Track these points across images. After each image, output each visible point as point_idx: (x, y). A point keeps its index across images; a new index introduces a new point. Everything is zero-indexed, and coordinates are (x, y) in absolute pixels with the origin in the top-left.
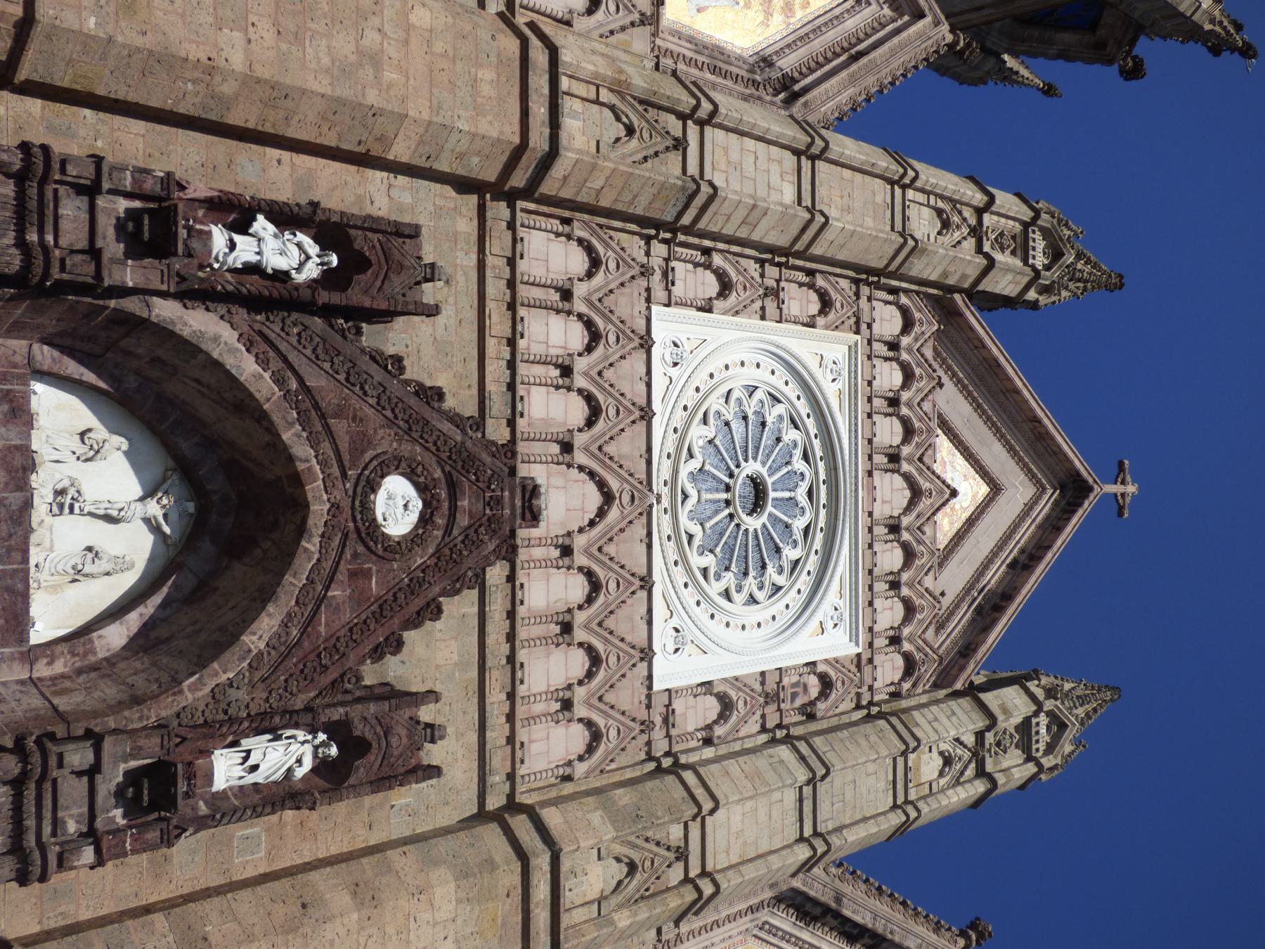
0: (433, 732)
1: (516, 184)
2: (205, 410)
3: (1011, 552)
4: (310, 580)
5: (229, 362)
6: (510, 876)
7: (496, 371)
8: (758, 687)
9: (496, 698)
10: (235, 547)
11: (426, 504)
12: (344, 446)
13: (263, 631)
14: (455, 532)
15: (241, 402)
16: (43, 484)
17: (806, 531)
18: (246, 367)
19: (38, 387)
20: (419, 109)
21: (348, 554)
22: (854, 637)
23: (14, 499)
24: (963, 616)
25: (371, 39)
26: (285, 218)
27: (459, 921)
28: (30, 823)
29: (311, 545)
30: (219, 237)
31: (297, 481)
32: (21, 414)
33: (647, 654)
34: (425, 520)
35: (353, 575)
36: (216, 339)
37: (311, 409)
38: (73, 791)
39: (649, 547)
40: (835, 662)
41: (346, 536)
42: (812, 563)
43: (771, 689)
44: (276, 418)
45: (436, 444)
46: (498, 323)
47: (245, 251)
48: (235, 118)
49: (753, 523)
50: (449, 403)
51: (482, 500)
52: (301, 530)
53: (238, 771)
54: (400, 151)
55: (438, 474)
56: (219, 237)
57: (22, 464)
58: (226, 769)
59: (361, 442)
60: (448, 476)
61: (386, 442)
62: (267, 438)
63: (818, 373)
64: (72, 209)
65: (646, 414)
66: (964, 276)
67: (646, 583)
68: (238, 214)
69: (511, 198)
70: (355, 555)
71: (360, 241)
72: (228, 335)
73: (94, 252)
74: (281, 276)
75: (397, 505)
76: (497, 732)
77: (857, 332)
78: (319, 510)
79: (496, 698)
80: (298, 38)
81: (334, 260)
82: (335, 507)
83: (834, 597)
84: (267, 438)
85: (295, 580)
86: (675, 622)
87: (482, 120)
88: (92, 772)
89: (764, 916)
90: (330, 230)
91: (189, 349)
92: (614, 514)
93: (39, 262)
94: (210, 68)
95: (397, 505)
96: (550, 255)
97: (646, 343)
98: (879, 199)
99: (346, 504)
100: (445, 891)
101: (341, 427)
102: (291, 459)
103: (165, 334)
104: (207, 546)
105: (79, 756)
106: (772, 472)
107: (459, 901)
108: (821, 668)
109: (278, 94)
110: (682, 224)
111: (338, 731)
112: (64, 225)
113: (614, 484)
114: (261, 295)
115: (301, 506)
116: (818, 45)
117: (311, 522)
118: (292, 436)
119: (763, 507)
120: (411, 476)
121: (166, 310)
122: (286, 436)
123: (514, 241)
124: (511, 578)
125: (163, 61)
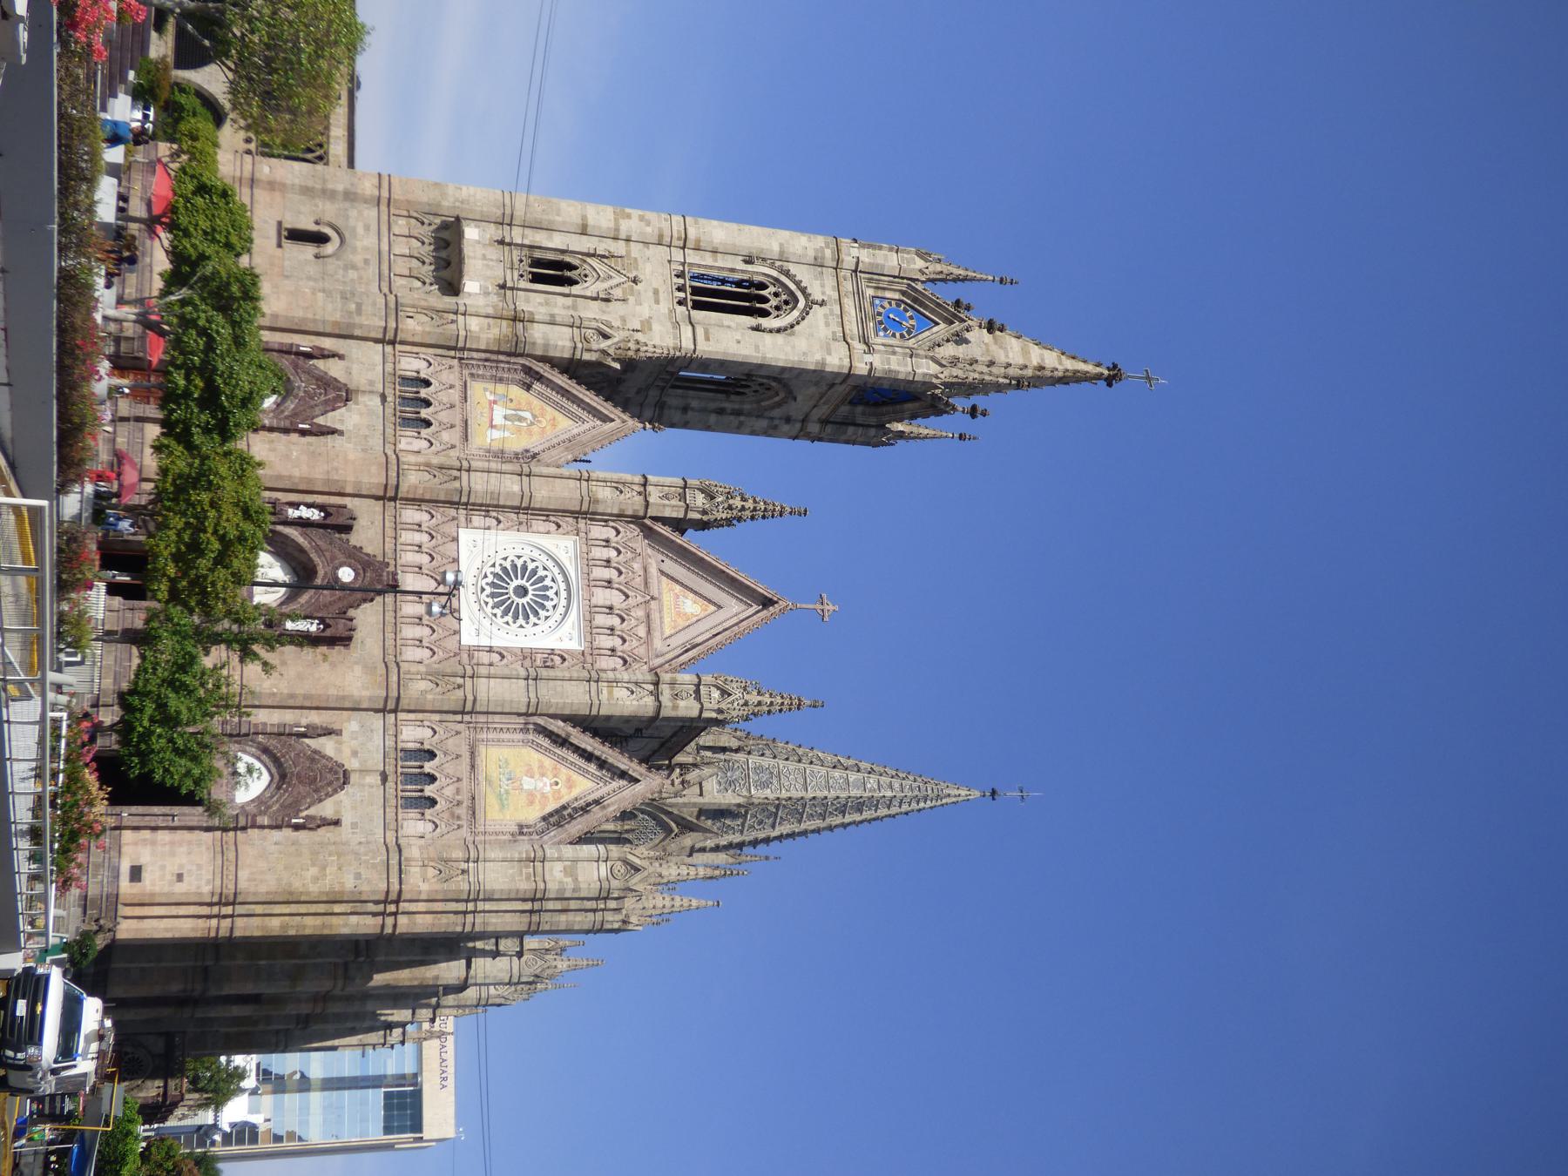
1: (389, 496)
2: (296, 554)
3: (720, 628)
6: (381, 669)
7: (389, 546)
9: (390, 636)
13: (304, 598)
15: (302, 550)
18: (301, 540)
20: (351, 478)
24: (679, 651)
26: (309, 506)
30: (290, 511)
33: (457, 632)
37: (319, 549)
40: (567, 651)
42: (557, 617)
43: (527, 655)
46: (390, 532)
48: (301, 487)
49: (524, 600)
54: (349, 490)
58: (289, 625)
65: (456, 560)
68: (296, 505)
69: (390, 499)
71: (330, 510)
75: (346, 575)
76: (390, 643)
87: (373, 478)
89: (531, 737)
90: (321, 508)
91: (286, 537)
94: (290, 477)
96: (411, 515)
97: (456, 539)
100: (358, 670)
103: (280, 534)
109: (310, 481)
110: (465, 505)
111: (322, 620)
114: (303, 523)
115: (316, 572)
116: (555, 441)
118: (313, 556)
121: (279, 528)
125: (280, 477)
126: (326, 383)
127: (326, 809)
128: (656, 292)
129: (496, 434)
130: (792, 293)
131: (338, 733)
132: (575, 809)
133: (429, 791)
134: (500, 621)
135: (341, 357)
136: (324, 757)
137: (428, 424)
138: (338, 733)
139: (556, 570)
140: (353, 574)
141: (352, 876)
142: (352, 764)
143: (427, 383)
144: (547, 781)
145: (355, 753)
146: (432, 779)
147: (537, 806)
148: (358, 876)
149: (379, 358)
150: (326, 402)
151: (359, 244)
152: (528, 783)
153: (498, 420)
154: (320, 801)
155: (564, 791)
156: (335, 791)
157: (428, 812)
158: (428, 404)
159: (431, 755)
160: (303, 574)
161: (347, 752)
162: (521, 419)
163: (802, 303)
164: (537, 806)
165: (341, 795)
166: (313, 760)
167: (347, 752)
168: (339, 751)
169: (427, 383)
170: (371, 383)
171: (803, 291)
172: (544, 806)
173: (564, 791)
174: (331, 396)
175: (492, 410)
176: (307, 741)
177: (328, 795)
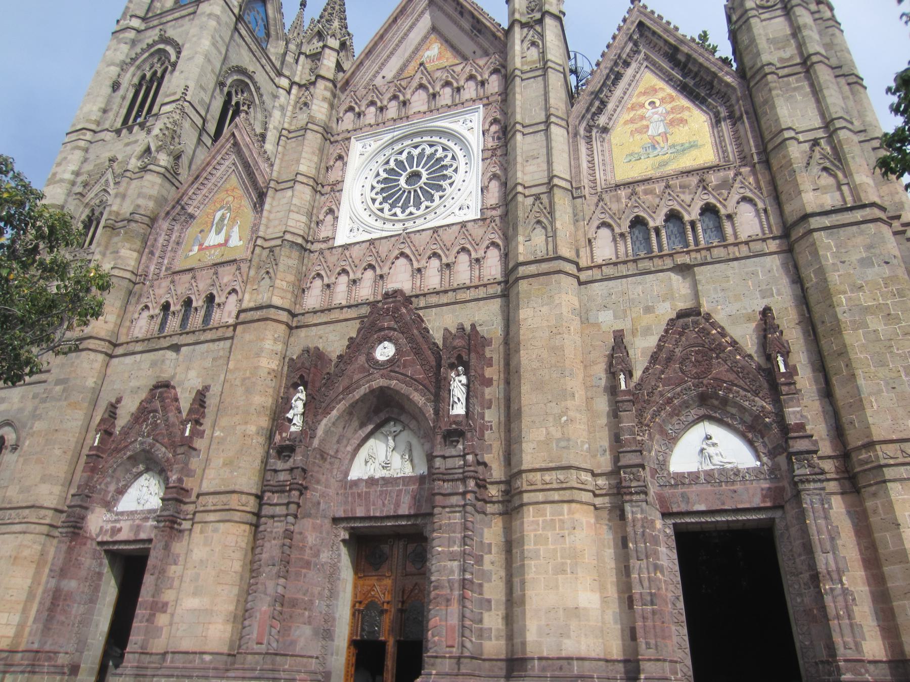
0: (461, 328)
4: (404, 382)
5: (333, 420)
8: (489, 161)
10: (402, 409)
11: (385, 340)
12: (362, 375)
14: (396, 326)
16: (380, 474)
17: (431, 146)
19: (349, 478)
21: (397, 369)
22: (476, 110)
23: (381, 482)
25: (238, 382)
27: (535, 305)
28: (456, 476)
29: (393, 383)
30: (293, 429)
31: (372, 391)
32: (356, 483)
33: (463, 224)
34: (390, 340)
35: (404, 367)
36: (326, 425)
37: (348, 389)
38: (450, 463)
39: (423, 230)
41: (391, 371)
42: (444, 141)
44: (351, 401)
45: (365, 339)
46: (336, 315)
47: (298, 421)
49: (425, 176)
50: (355, 336)
51: (393, 314)
52: (388, 388)
53: (459, 404)
55: (375, 336)
56: (293, 429)
57: (372, 481)
59: (362, 369)
60: (376, 332)
61: (362, 359)
62: (360, 403)
63: (366, 155)
64: (282, 477)
66: (326, 88)
67: (435, 230)
70: (398, 366)
72: (325, 421)
73: (291, 470)
74: (305, 405)
75: (385, 352)
77: (350, 138)
78: (382, 382)
79: (468, 295)
80: (238, 408)
81: (301, 388)
82: (382, 376)
83: (456, 125)
84: (360, 403)
85: (403, 388)
86: (457, 211)
88: (444, 457)
92: (407, 251)
93: (295, 486)
95: (385, 352)
98: (294, 145)
99: (381, 372)
101: (356, 377)
102: (365, 394)
104: (403, 418)
105: (438, 462)
106: (405, 170)
107: (528, 307)
108: (487, 127)
112: (286, 478)
113: (397, 252)
115: (382, 389)
117: (386, 385)
118: (358, 394)
119: (419, 172)
120: (373, 348)
122: (357, 397)
123: (308, 312)
124: (424, 295)
126: (143, 413)
127: (746, 336)
128: (127, 144)
129: (235, 241)
130: (152, 55)
131: (619, 337)
132: (684, 76)
133: (692, 214)
134: (449, 190)
135: (119, 400)
136: (660, 348)
137: (210, 299)
138: (619, 337)
139: (388, 152)
140: (386, 343)
141: (869, 271)
142: (666, 311)
143: (166, 307)
144: (648, 111)
145: (648, 310)
146: (673, 217)
147: (685, 115)
148: (866, 262)
149: (128, 360)
150: (164, 408)
151: (16, 407)
152: (656, 129)
153: (220, 239)
154: (734, 343)
155: (661, 95)
156: (714, 325)
157: (723, 211)
158: (188, 303)
159: (638, 222)
160: (383, 411)
161: (647, 319)
162: (222, 218)
163: (161, 46)
164: (685, 115)
165: (720, 317)
166: (669, 360)
167: (647, 319)
168: (647, 331)
169: (166, 307)
170: (154, 364)
171: (150, 46)
172: (688, 108)
173: (661, 95)
174: (157, 404)
175: (208, 248)
176: (638, 374)
177: (723, 334)
